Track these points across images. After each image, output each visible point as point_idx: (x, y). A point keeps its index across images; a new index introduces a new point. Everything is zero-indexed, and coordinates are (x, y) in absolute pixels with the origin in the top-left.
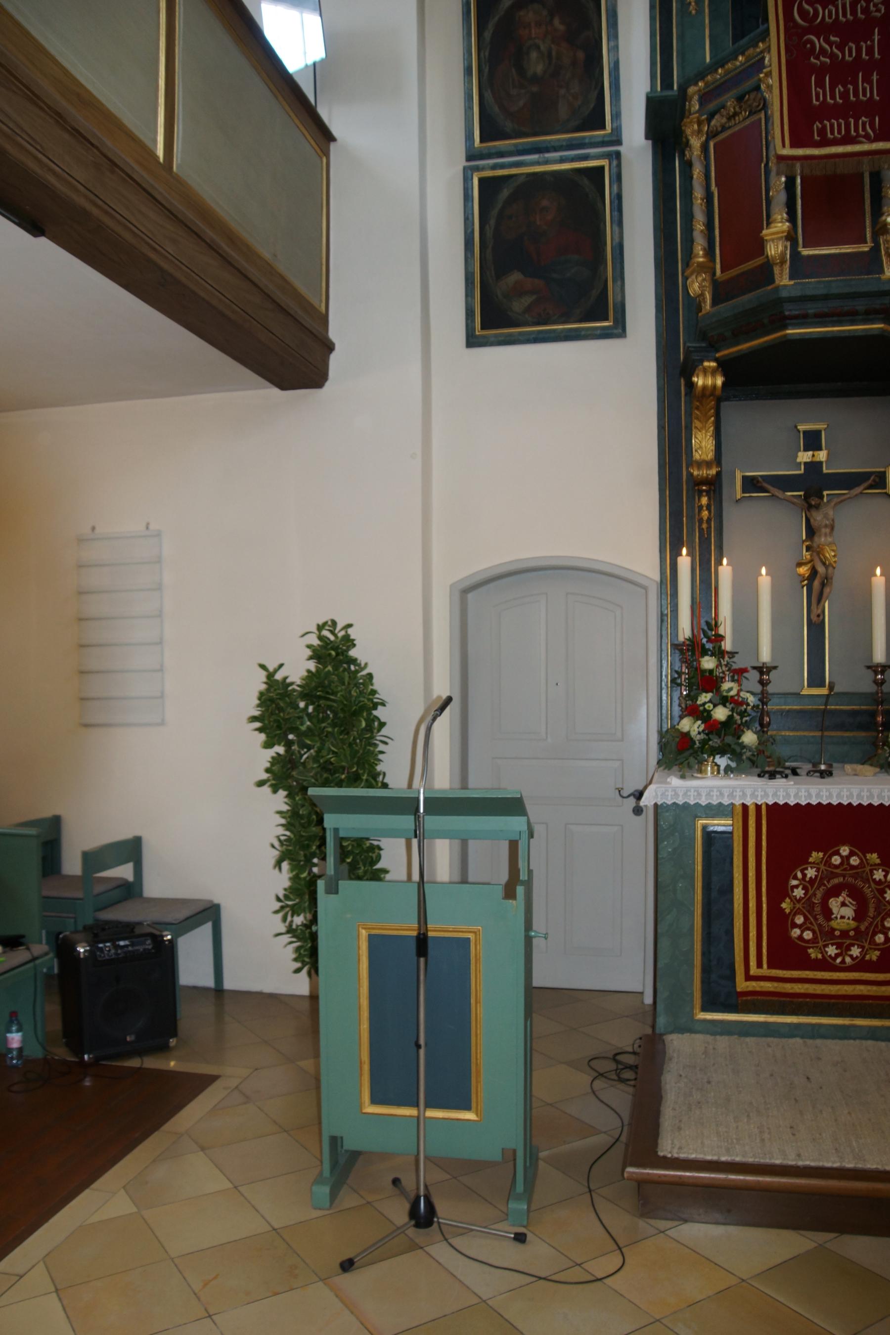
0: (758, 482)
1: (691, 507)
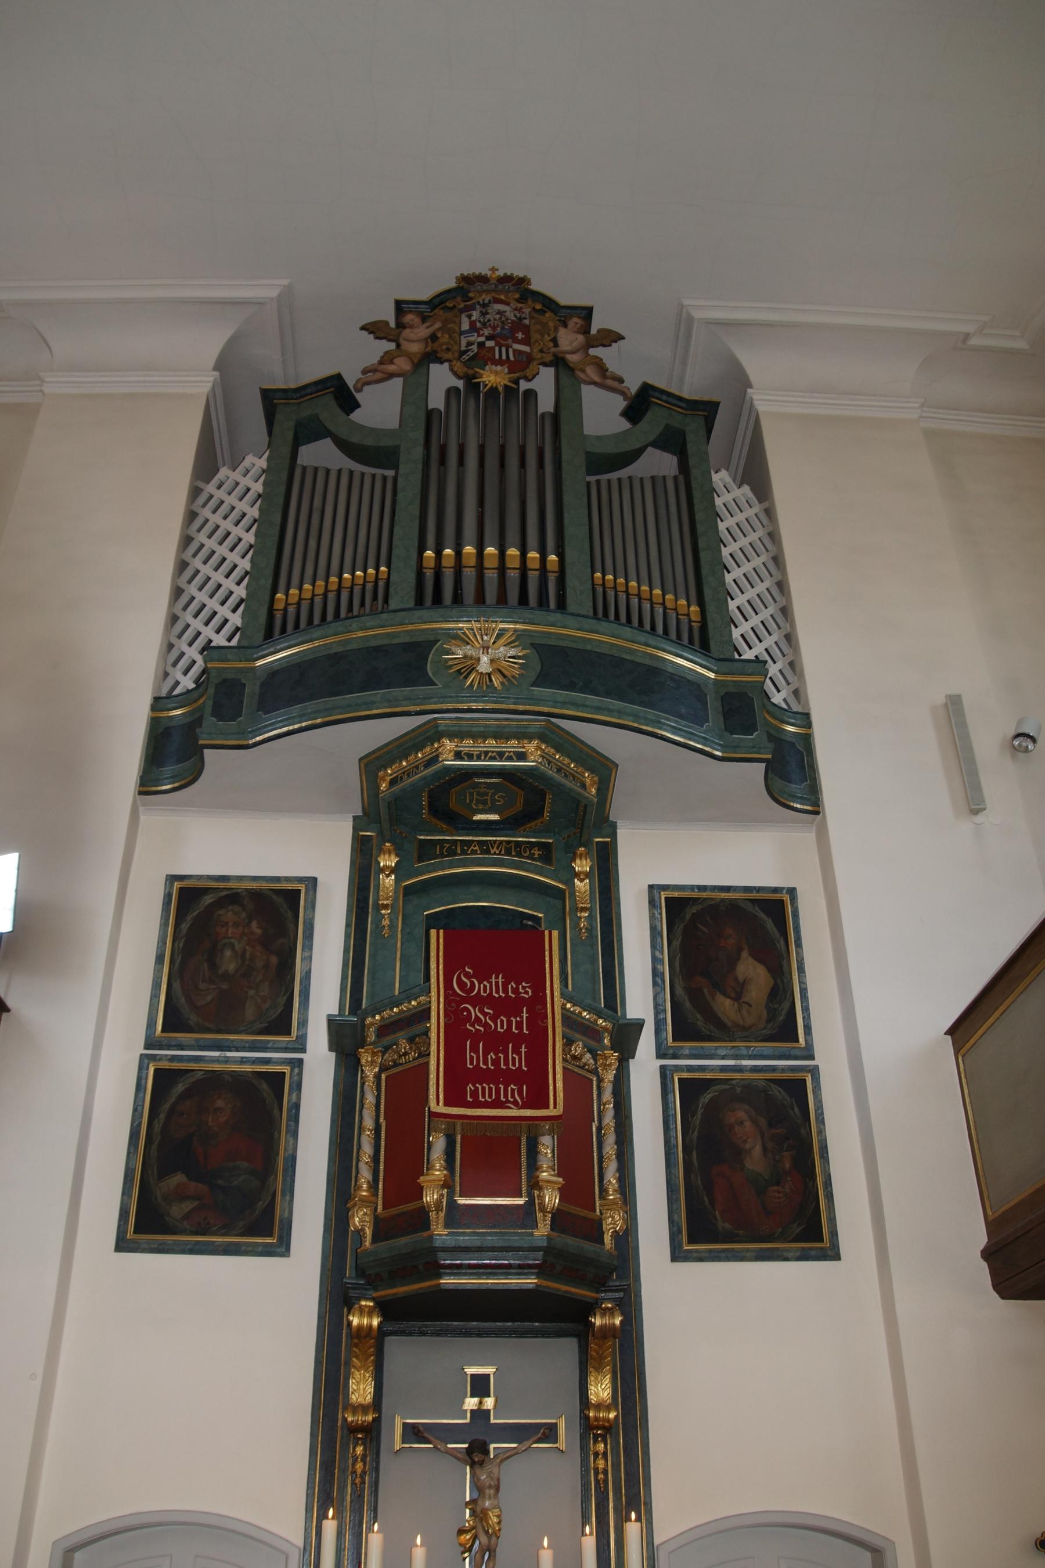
0: (419, 1431)
1: (345, 1456)
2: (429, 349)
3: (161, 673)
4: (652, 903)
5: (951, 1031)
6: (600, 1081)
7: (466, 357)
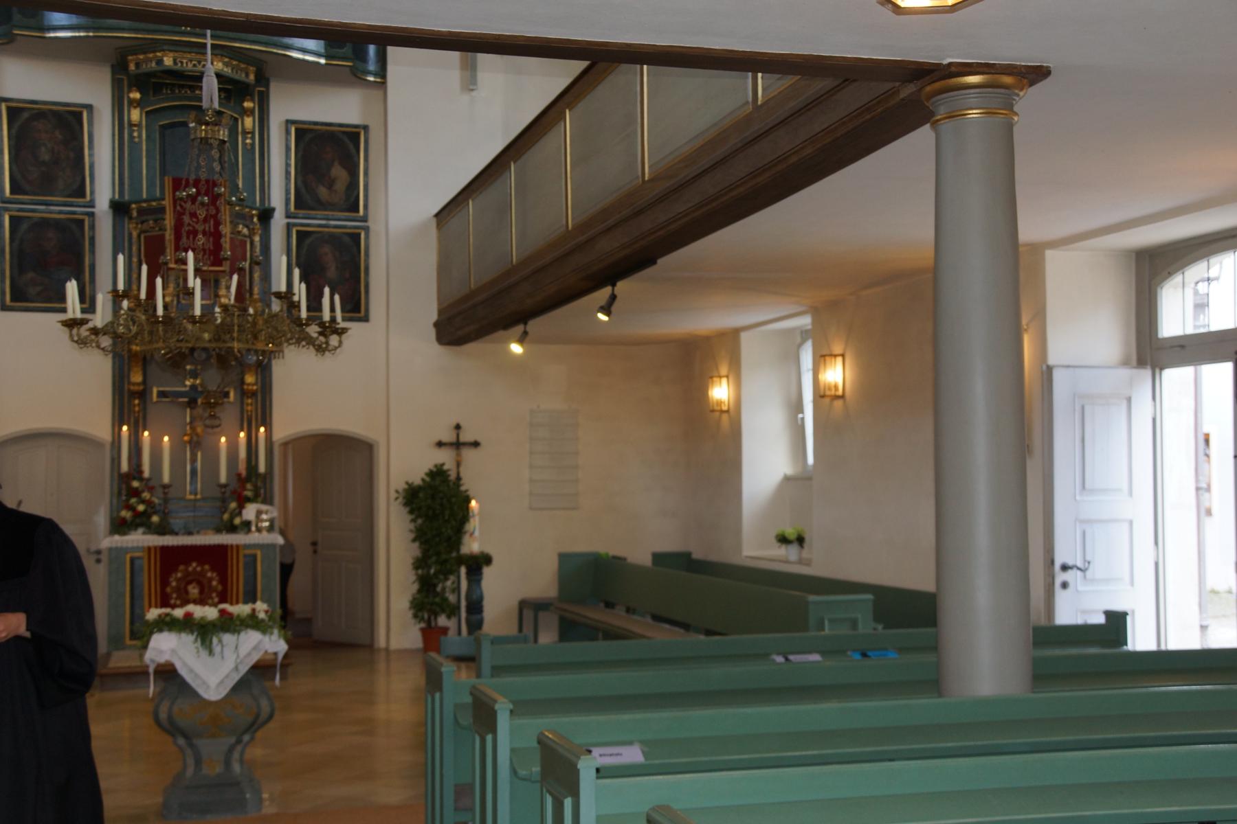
1: (129, 404)
4: (288, 132)
5: (437, 215)
6: (252, 243)
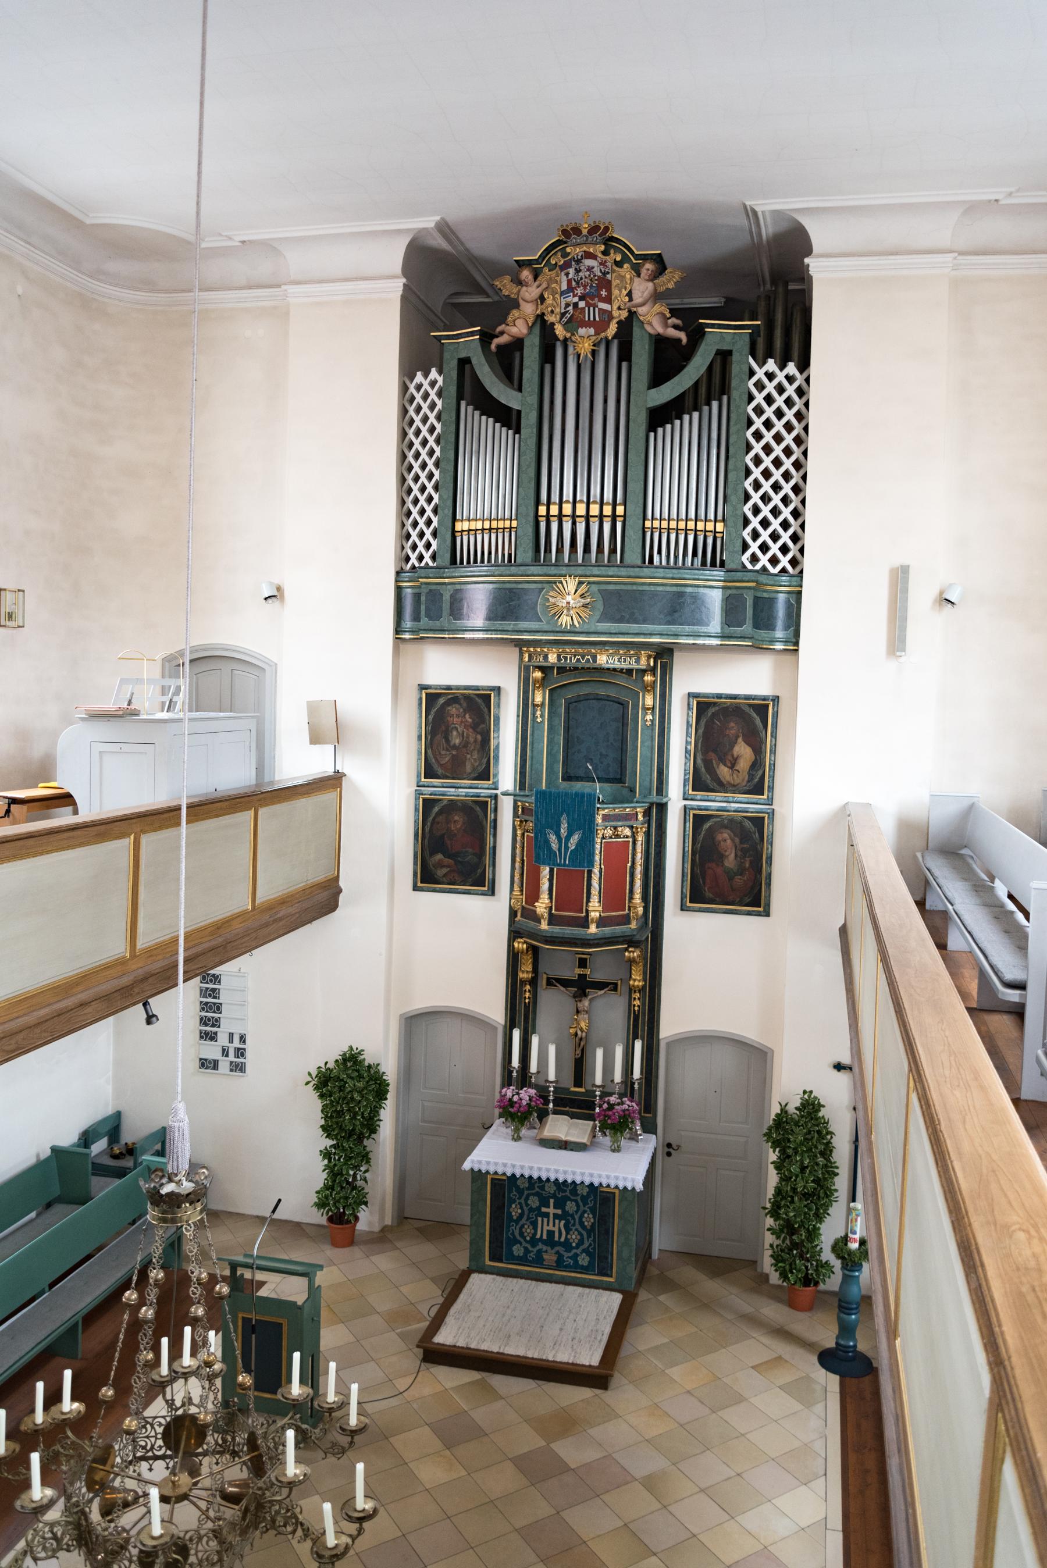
2: (538, 312)
3: (399, 546)
4: (689, 708)
7: (565, 320)
